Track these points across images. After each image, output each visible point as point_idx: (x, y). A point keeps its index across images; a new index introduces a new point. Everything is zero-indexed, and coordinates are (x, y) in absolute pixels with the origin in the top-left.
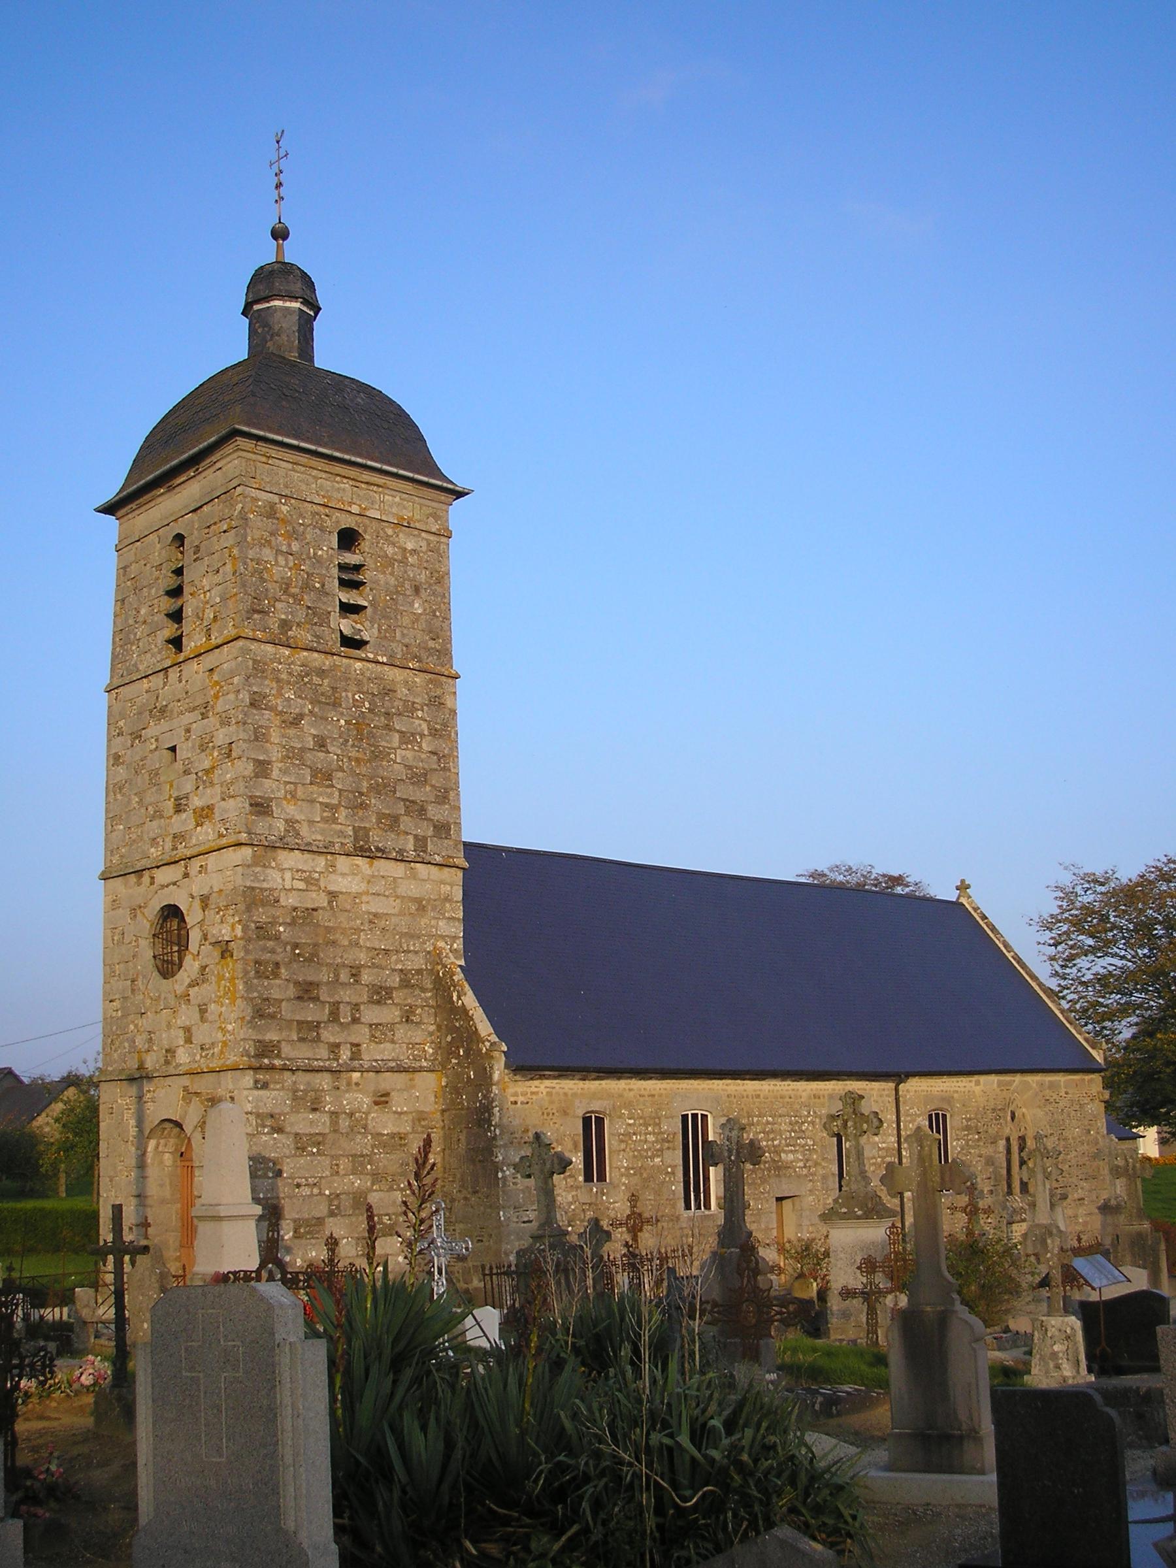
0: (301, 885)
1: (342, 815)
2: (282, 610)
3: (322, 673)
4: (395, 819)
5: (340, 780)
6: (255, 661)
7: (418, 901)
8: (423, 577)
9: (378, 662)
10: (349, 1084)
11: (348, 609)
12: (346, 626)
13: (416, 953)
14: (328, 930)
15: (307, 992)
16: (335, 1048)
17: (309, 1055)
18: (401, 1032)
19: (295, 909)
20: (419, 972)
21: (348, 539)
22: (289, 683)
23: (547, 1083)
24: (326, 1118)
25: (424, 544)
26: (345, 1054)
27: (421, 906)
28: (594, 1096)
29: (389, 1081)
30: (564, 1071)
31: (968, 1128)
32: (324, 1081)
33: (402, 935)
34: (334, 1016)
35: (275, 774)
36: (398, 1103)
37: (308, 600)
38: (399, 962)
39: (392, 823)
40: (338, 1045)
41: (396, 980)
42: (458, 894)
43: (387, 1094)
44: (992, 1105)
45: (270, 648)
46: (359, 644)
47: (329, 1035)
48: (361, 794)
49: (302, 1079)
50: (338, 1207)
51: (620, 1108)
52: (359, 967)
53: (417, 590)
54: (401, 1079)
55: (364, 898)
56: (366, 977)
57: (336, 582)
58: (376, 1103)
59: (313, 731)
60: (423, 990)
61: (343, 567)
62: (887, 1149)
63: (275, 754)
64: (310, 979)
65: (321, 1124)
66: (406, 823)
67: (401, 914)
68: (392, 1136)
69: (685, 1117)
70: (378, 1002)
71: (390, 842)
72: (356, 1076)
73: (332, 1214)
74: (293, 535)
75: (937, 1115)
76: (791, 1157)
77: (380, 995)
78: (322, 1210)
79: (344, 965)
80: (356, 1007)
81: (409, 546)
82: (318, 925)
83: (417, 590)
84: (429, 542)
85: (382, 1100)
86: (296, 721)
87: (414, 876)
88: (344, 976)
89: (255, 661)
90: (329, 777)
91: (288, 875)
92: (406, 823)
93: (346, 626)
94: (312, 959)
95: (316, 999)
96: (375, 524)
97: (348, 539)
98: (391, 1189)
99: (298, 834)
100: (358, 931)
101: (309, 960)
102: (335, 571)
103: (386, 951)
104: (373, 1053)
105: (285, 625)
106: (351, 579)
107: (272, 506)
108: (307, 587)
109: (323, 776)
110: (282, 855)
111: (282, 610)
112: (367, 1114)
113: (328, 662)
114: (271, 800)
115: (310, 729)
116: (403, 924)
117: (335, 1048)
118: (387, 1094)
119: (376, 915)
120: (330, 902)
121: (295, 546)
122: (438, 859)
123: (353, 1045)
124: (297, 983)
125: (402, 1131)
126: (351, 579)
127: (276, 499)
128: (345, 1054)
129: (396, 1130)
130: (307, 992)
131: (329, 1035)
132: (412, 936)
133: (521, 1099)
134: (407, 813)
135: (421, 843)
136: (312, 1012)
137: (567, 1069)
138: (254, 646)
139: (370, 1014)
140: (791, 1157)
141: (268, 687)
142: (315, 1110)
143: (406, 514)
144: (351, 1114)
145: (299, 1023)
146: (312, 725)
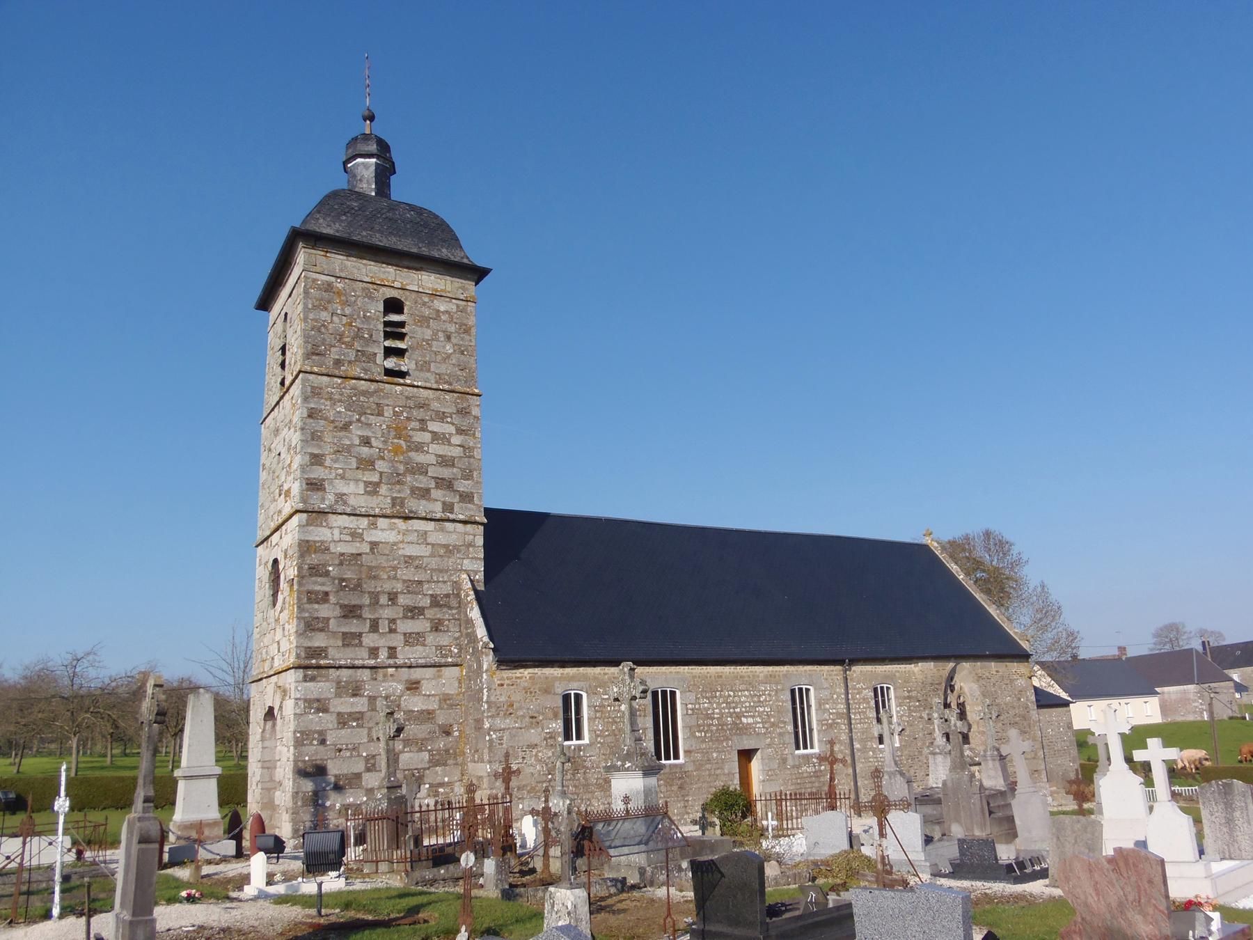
0: (349, 538)
1: (383, 489)
2: (334, 354)
3: (365, 393)
4: (428, 491)
5: (381, 466)
6: (313, 387)
7: (446, 546)
8: (452, 328)
9: (414, 386)
10: (385, 676)
11: (389, 352)
12: (391, 363)
13: (445, 582)
14: (370, 568)
15: (350, 612)
16: (374, 652)
17: (351, 656)
18: (430, 639)
19: (342, 554)
20: (447, 596)
21: (394, 306)
22: (340, 401)
23: (530, 670)
24: (364, 701)
25: (454, 307)
26: (383, 655)
27: (449, 550)
28: (572, 679)
29: (417, 674)
30: (563, 664)
31: (909, 697)
32: (365, 675)
33: (432, 570)
34: (374, 627)
35: (328, 463)
36: (427, 688)
37: (357, 345)
38: (429, 589)
39: (425, 494)
40: (377, 649)
41: (426, 602)
42: (480, 541)
43: (418, 682)
44: (930, 680)
45: (325, 379)
46: (402, 375)
47: (369, 640)
48: (398, 475)
49: (345, 674)
50: (374, 765)
51: (596, 687)
52: (396, 593)
53: (449, 338)
54: (430, 672)
55: (401, 546)
56: (402, 600)
57: (382, 334)
58: (408, 689)
59: (359, 433)
60: (451, 608)
61: (386, 324)
62: (837, 713)
63: (328, 449)
64: (353, 603)
65: (360, 704)
66: (435, 494)
67: (432, 555)
68: (421, 712)
69: (793, 691)
70: (413, 618)
71: (422, 507)
72: (391, 670)
73: (368, 770)
74: (346, 303)
75: (801, 689)
76: (750, 720)
77: (414, 612)
78: (359, 767)
79: (384, 592)
80: (393, 621)
81: (442, 309)
82: (362, 565)
83: (449, 338)
84: (458, 306)
85: (413, 686)
86: (346, 427)
87: (442, 530)
88: (383, 600)
89: (313, 387)
90: (372, 463)
91: (336, 532)
92: (435, 494)
93: (391, 363)
94: (358, 587)
95: (360, 617)
96: (414, 296)
97: (394, 306)
98: (420, 750)
99: (345, 503)
100: (395, 568)
101: (354, 589)
102: (381, 327)
103: (420, 582)
104: (407, 654)
105: (338, 363)
106: (395, 331)
107: (330, 284)
108: (358, 336)
109: (367, 464)
110: (332, 517)
111: (334, 354)
112: (400, 697)
113: (373, 386)
114: (324, 480)
115: (357, 432)
116: (434, 563)
117: (374, 652)
118: (418, 682)
119: (410, 557)
120: (372, 549)
121: (348, 311)
122: (461, 517)
123: (390, 648)
124: (342, 606)
125: (431, 708)
126: (395, 331)
127: (333, 279)
128: (383, 655)
129: (424, 708)
130: (350, 612)
131: (369, 640)
132: (441, 571)
133: (507, 682)
134: (437, 487)
135: (448, 507)
136: (353, 626)
137: (513, 662)
138: (311, 377)
139: (406, 626)
140: (750, 720)
141: (324, 405)
142: (354, 695)
143: (439, 287)
144: (387, 698)
145: (344, 634)
146: (359, 428)
